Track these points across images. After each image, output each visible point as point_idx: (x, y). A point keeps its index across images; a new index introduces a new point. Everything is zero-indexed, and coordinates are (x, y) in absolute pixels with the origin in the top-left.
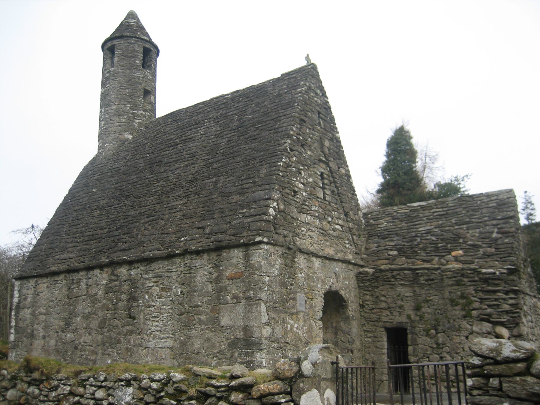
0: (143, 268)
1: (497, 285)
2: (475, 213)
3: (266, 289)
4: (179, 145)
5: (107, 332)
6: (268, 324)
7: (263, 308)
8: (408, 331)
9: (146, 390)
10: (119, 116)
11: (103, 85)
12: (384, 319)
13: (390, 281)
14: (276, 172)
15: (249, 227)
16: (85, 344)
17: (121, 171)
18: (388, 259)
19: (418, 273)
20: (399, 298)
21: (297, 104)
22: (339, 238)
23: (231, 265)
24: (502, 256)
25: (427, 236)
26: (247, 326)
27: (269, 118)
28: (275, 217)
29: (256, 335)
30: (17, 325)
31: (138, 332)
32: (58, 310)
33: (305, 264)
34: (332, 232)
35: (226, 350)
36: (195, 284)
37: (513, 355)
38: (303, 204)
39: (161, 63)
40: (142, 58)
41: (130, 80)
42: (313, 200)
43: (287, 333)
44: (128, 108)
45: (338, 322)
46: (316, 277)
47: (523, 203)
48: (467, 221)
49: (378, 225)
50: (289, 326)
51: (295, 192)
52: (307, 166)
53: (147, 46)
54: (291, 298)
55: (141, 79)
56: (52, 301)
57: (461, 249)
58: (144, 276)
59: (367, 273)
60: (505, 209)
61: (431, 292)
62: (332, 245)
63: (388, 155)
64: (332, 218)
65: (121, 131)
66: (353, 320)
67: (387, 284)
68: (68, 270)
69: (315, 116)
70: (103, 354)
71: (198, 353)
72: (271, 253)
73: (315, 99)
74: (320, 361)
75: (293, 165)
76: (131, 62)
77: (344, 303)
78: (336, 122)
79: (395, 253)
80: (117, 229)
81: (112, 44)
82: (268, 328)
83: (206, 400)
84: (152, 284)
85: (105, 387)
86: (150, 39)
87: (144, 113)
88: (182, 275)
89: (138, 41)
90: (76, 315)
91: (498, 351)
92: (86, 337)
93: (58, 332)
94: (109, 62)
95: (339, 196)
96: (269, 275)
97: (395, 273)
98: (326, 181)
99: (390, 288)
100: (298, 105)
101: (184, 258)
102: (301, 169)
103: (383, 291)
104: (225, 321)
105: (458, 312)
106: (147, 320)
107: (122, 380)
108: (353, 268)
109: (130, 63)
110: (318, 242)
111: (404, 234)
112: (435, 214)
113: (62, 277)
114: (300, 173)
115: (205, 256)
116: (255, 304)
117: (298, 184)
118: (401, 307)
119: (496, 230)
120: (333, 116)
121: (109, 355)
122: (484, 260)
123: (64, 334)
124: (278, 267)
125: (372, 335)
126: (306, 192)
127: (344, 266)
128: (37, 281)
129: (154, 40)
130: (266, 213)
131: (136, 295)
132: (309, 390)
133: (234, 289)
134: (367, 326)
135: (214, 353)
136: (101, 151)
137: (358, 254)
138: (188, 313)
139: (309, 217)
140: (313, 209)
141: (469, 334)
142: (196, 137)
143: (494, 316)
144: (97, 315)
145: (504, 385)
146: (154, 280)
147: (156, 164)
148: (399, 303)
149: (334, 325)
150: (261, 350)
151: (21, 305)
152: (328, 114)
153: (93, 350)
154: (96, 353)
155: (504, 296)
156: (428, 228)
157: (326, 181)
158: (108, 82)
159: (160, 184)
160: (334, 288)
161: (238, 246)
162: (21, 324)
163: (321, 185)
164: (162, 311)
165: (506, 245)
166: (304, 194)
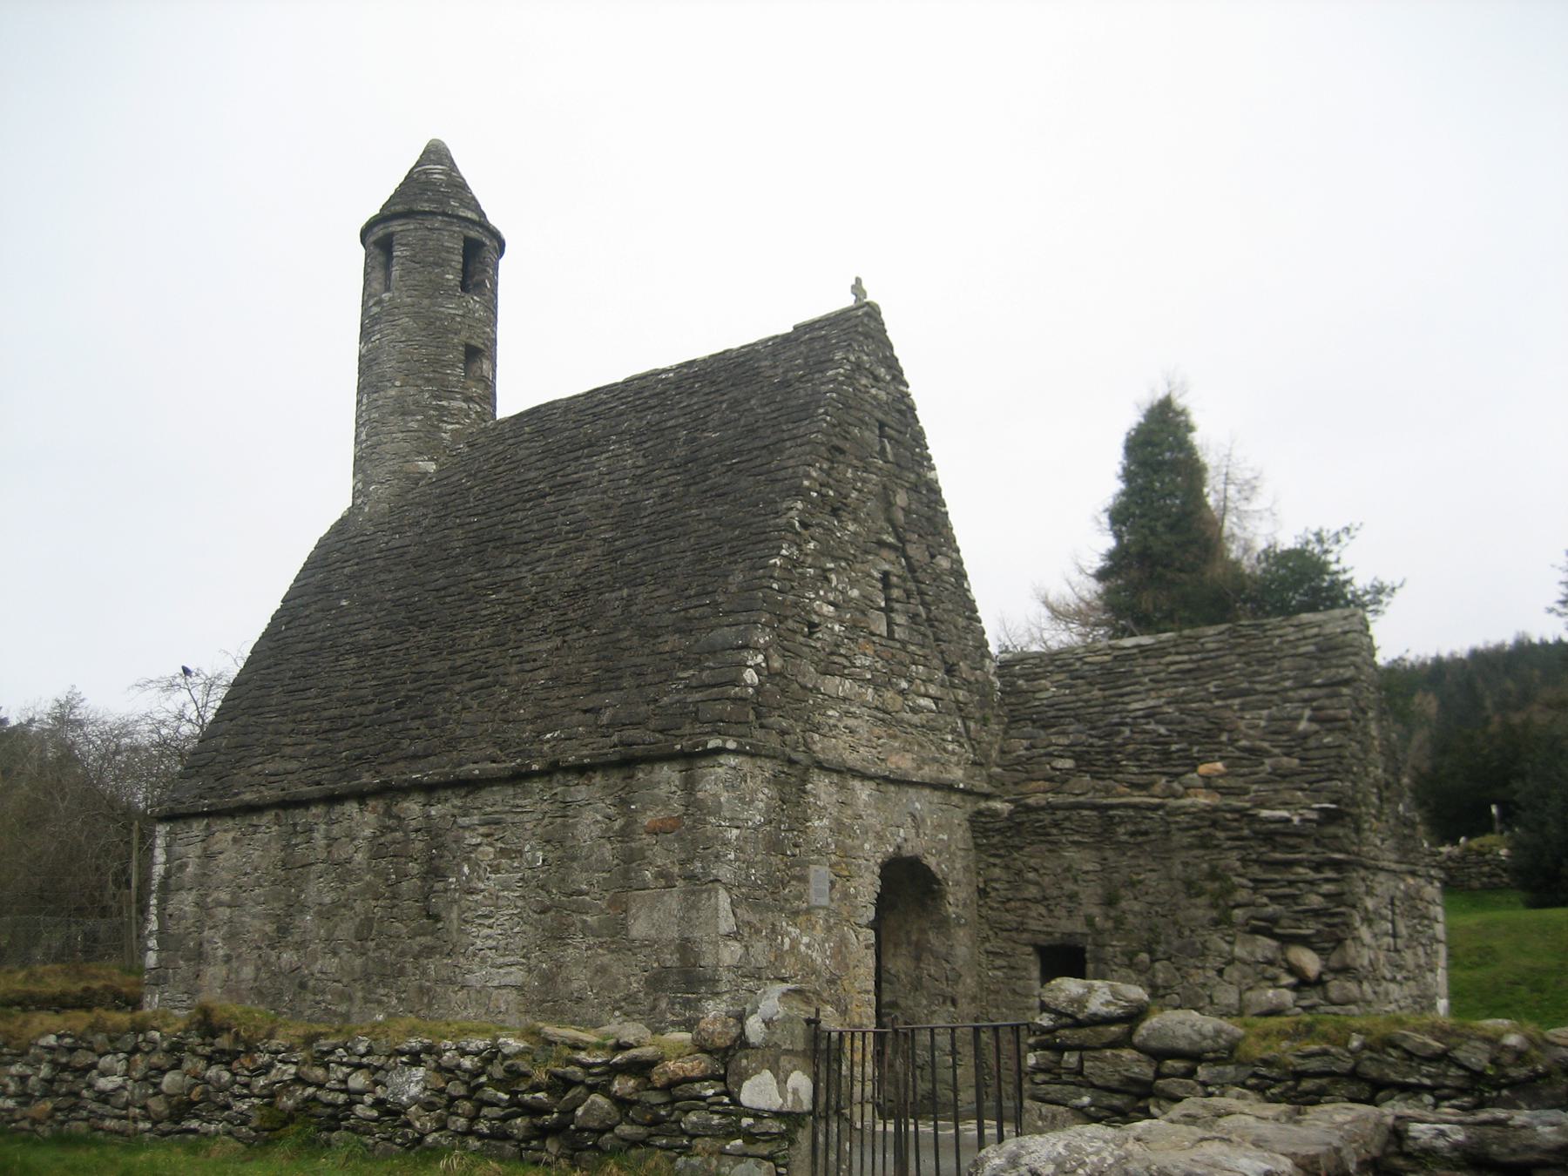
0: (458, 802)
1: (1294, 848)
2: (1262, 670)
3: (732, 856)
4: (549, 499)
5: (375, 950)
6: (734, 936)
7: (724, 899)
8: (1087, 955)
9: (450, 1072)
10: (403, 414)
11: (365, 334)
12: (1034, 925)
13: (1049, 835)
14: (765, 582)
15: (696, 713)
16: (324, 977)
17: (408, 557)
18: (1050, 779)
19: (1112, 818)
20: (1069, 875)
21: (822, 411)
22: (929, 728)
23: (655, 802)
24: (1312, 777)
25: (1148, 723)
26: (688, 940)
27: (758, 443)
28: (759, 689)
29: (708, 960)
30: (162, 931)
31: (446, 951)
32: (259, 895)
33: (831, 795)
34: (908, 716)
35: (641, 995)
36: (575, 843)
37: (1104, 1010)
38: (832, 653)
39: (510, 273)
40: (459, 266)
41: (431, 323)
42: (861, 640)
43: (782, 956)
44: (427, 396)
45: (923, 931)
46: (860, 827)
47: (1562, 583)
48: (1243, 689)
49: (1034, 692)
50: (787, 940)
51: (813, 626)
52: (846, 560)
53: (473, 234)
54: (793, 877)
55: (458, 319)
56: (246, 874)
57: (1222, 758)
58: (460, 821)
59: (995, 814)
60: (1334, 662)
61: (1141, 862)
62: (908, 747)
63: (1128, 476)
64: (911, 682)
65: (409, 453)
66: (959, 925)
67: (1042, 841)
68: (284, 801)
69: (871, 436)
70: (366, 1001)
71: (579, 1000)
72: (745, 775)
73: (873, 391)
74: (780, 1016)
75: (809, 560)
76: (433, 277)
77: (936, 887)
78: (928, 441)
79: (1068, 764)
80: (399, 706)
81: (386, 231)
82: (736, 947)
83: (566, 1092)
84: (479, 840)
85: (367, 1066)
86: (483, 215)
87: (465, 405)
88: (546, 821)
89: (451, 224)
90: (304, 908)
91: (1080, 1002)
92: (327, 961)
93: (260, 948)
94: (378, 274)
95: (932, 626)
96: (740, 824)
97: (1060, 814)
98: (896, 593)
99: (1050, 851)
100: (826, 413)
101: (550, 781)
102: (830, 570)
103: (1031, 857)
104: (639, 928)
105: (1200, 911)
106: (467, 922)
107: (402, 1053)
108: (963, 800)
109: (430, 281)
110: (869, 741)
111: (1095, 717)
112: (1172, 668)
113: (269, 817)
114: (829, 581)
115: (598, 779)
116: (705, 890)
117: (820, 606)
118: (1072, 897)
119: (1307, 713)
120: (921, 428)
121: (380, 1002)
122: (1272, 786)
123: (274, 954)
124: (761, 805)
125: (1004, 964)
126: (841, 623)
127: (937, 796)
128: (208, 826)
129: (494, 219)
130: (736, 682)
131: (442, 864)
132: (756, 1072)
133: (662, 856)
134: (993, 942)
135: (616, 1001)
136: (359, 501)
137: (981, 765)
138: (559, 907)
139: (847, 683)
140: (858, 663)
141: (1225, 963)
142: (587, 479)
143: (1284, 922)
144: (352, 908)
145: (1086, 1064)
146: (482, 830)
147: (491, 545)
148: (1069, 886)
149: (914, 938)
150: (717, 994)
151: (173, 880)
152: (907, 426)
153: (343, 991)
154: (350, 999)
155: (1311, 875)
156: (1152, 703)
157: (896, 593)
158: (377, 328)
159: (500, 596)
160: (908, 851)
161: (670, 758)
162: (173, 928)
163: (883, 604)
164: (501, 902)
165: (1325, 752)
166: (837, 627)
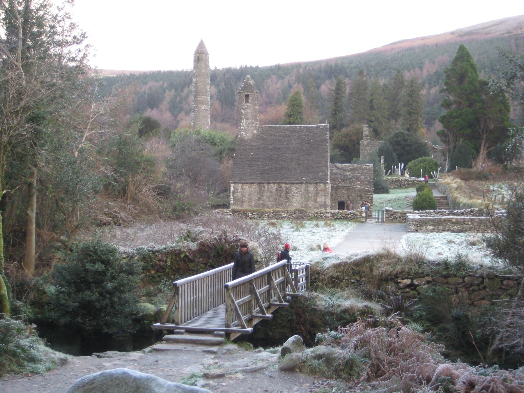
90: (264, 196)
104: (318, 200)
115: (312, 184)
